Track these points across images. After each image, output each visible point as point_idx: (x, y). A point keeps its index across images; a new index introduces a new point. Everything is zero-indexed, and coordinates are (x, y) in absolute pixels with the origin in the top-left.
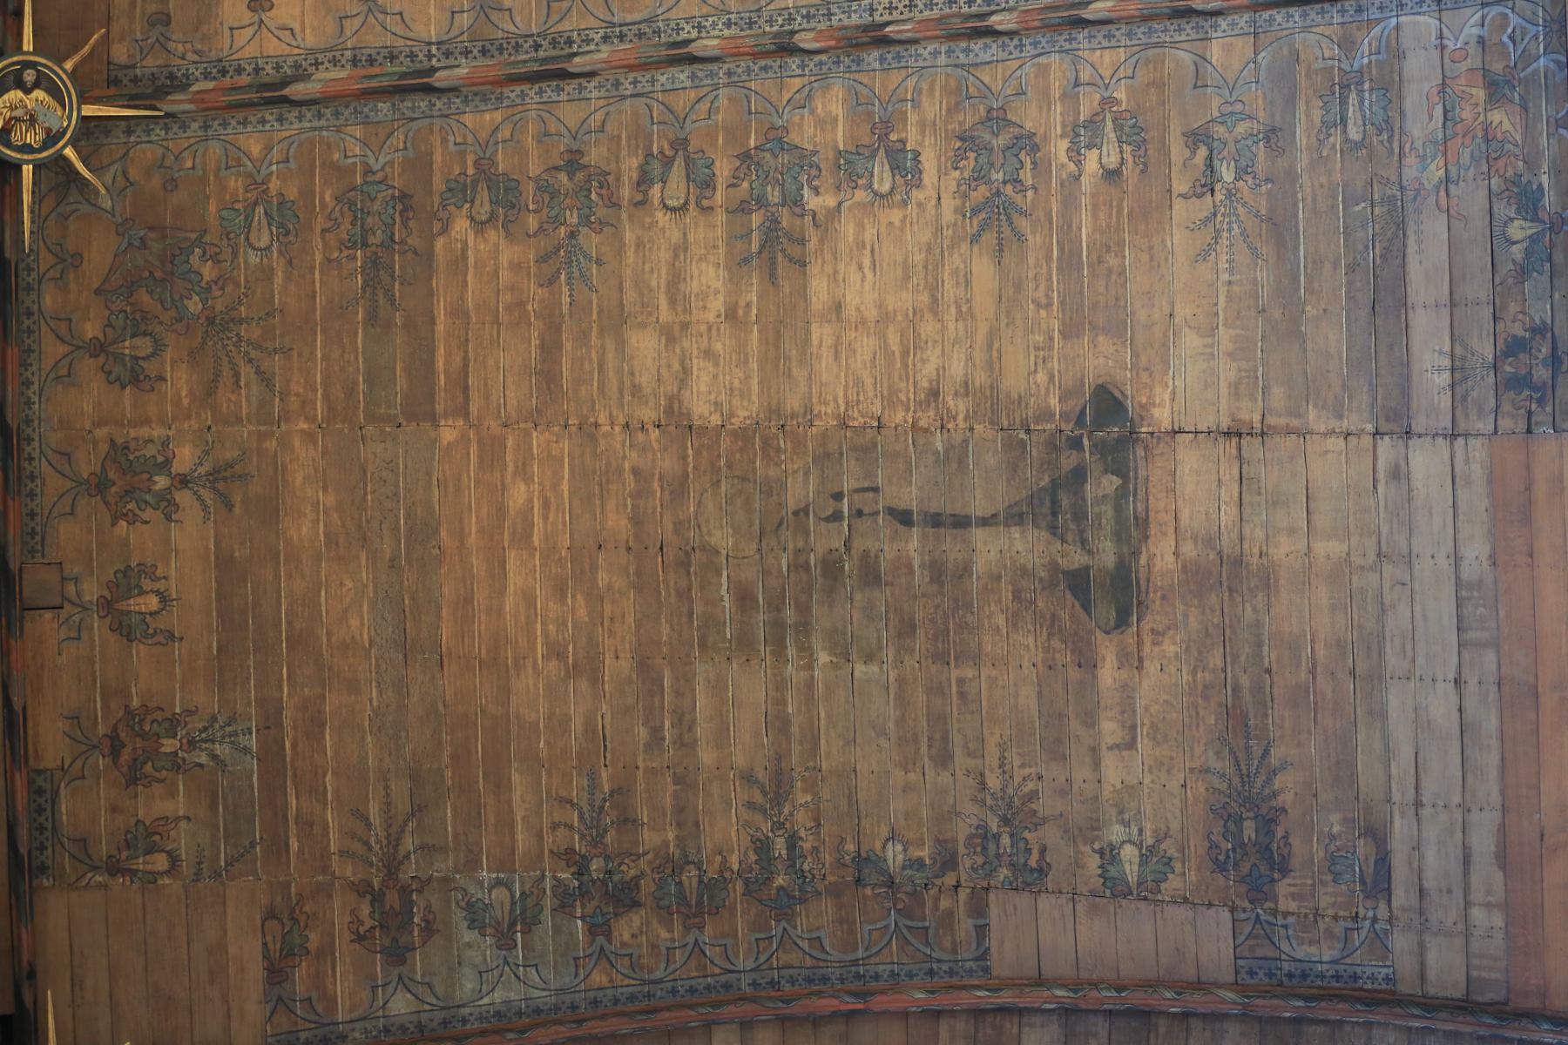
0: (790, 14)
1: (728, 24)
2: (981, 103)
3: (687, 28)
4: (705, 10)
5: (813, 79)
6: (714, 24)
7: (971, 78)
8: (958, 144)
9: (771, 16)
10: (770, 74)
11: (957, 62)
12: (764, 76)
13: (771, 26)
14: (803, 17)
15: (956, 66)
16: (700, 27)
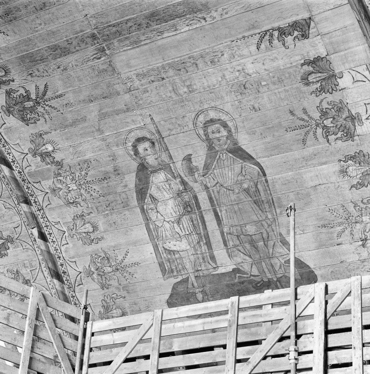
0: (33, 195)
1: (20, 172)
2: (30, 276)
3: (11, 157)
4: (20, 162)
5: (16, 208)
6: (17, 167)
7: (37, 270)
8: (15, 271)
9: (30, 188)
10: (11, 192)
11: (41, 263)
12: (9, 190)
13: (27, 188)
14: (34, 200)
15: (40, 263)
16: (14, 162)
